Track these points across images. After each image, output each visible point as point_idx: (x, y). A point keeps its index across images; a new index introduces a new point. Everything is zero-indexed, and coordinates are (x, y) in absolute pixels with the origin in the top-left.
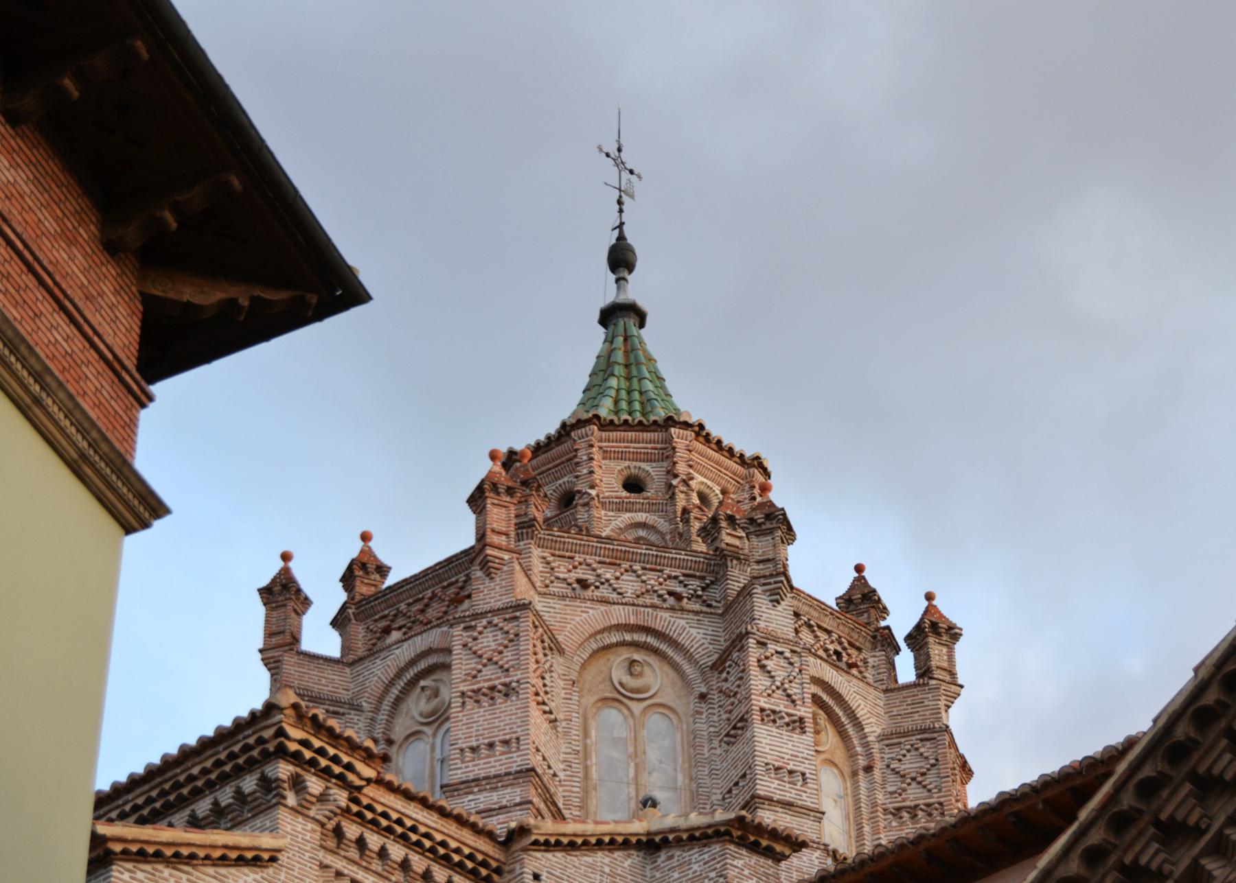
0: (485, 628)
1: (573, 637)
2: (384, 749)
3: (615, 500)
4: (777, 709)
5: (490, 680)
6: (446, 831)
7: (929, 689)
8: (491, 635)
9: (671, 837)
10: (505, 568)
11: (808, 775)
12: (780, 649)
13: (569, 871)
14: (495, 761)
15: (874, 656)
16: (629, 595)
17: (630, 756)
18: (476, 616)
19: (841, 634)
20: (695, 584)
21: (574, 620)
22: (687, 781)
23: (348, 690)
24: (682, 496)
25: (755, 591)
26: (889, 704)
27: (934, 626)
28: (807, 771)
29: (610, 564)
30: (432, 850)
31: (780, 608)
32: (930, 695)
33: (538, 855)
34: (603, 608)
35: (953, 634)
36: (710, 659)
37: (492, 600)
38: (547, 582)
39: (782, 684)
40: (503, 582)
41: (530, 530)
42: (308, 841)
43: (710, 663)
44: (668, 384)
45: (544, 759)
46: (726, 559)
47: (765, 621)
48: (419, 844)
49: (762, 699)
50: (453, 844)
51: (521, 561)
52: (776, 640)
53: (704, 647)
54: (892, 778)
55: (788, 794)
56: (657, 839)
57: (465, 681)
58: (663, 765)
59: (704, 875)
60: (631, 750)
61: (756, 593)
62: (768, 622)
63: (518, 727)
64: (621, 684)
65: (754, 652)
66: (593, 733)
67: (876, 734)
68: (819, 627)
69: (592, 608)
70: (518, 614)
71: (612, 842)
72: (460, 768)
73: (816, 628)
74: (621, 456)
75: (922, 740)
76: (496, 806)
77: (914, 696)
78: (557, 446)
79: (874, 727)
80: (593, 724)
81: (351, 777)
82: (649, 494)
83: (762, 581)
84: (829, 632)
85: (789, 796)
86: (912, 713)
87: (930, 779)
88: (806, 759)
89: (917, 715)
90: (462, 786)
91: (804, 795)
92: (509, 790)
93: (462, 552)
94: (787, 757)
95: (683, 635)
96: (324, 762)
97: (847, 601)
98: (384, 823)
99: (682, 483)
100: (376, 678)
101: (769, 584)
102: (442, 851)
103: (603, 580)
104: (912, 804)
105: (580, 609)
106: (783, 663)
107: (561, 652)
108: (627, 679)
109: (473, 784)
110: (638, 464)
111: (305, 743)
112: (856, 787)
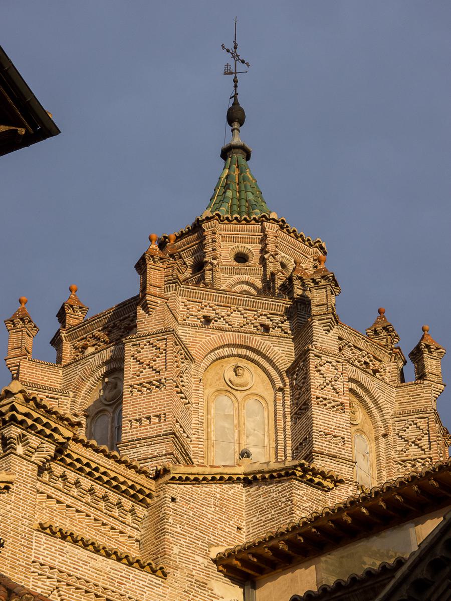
1: (201, 352)
3: (229, 267)
4: (327, 397)
5: (148, 378)
7: (424, 387)
8: (148, 350)
9: (258, 476)
12: (329, 360)
13: (194, 496)
14: (150, 428)
16: (236, 326)
17: (236, 426)
19: (369, 352)
20: (278, 319)
21: (201, 341)
23: (61, 384)
24: (271, 265)
25: (314, 324)
26: (398, 396)
28: (345, 436)
30: (108, 482)
31: (330, 334)
32: (424, 390)
33: (175, 486)
34: (219, 333)
36: (286, 366)
37: (150, 328)
38: (185, 317)
39: (330, 382)
40: (157, 317)
41: (174, 285)
42: (29, 477)
43: (285, 369)
45: (181, 427)
46: (297, 304)
47: (320, 343)
48: (99, 478)
49: (318, 391)
50: (122, 479)
51: (169, 304)
53: (282, 358)
54: (400, 441)
55: (333, 451)
56: (250, 477)
58: (256, 432)
59: (278, 500)
60: (236, 422)
61: (315, 325)
62: (322, 343)
63: (165, 407)
64: (230, 381)
66: (213, 411)
67: (390, 414)
68: (355, 347)
69: (213, 334)
70: (166, 337)
71: (221, 478)
72: (129, 432)
73: (353, 348)
74: (234, 240)
75: (419, 418)
76: (151, 456)
77: (415, 390)
79: (389, 412)
80: (213, 405)
81: (56, 436)
82: (250, 264)
83: (319, 317)
84: (361, 350)
86: (413, 401)
88: (345, 429)
89: (416, 402)
90: (129, 444)
91: (343, 451)
92: (159, 445)
93: (132, 298)
94: (333, 427)
95: (269, 351)
96: (40, 427)
98: (78, 465)
99: (271, 257)
100: (77, 377)
101: (324, 319)
102: (115, 483)
103: (220, 316)
105: (205, 334)
106: (332, 369)
107: (193, 360)
109: (136, 442)
110: (244, 245)
111: (27, 415)
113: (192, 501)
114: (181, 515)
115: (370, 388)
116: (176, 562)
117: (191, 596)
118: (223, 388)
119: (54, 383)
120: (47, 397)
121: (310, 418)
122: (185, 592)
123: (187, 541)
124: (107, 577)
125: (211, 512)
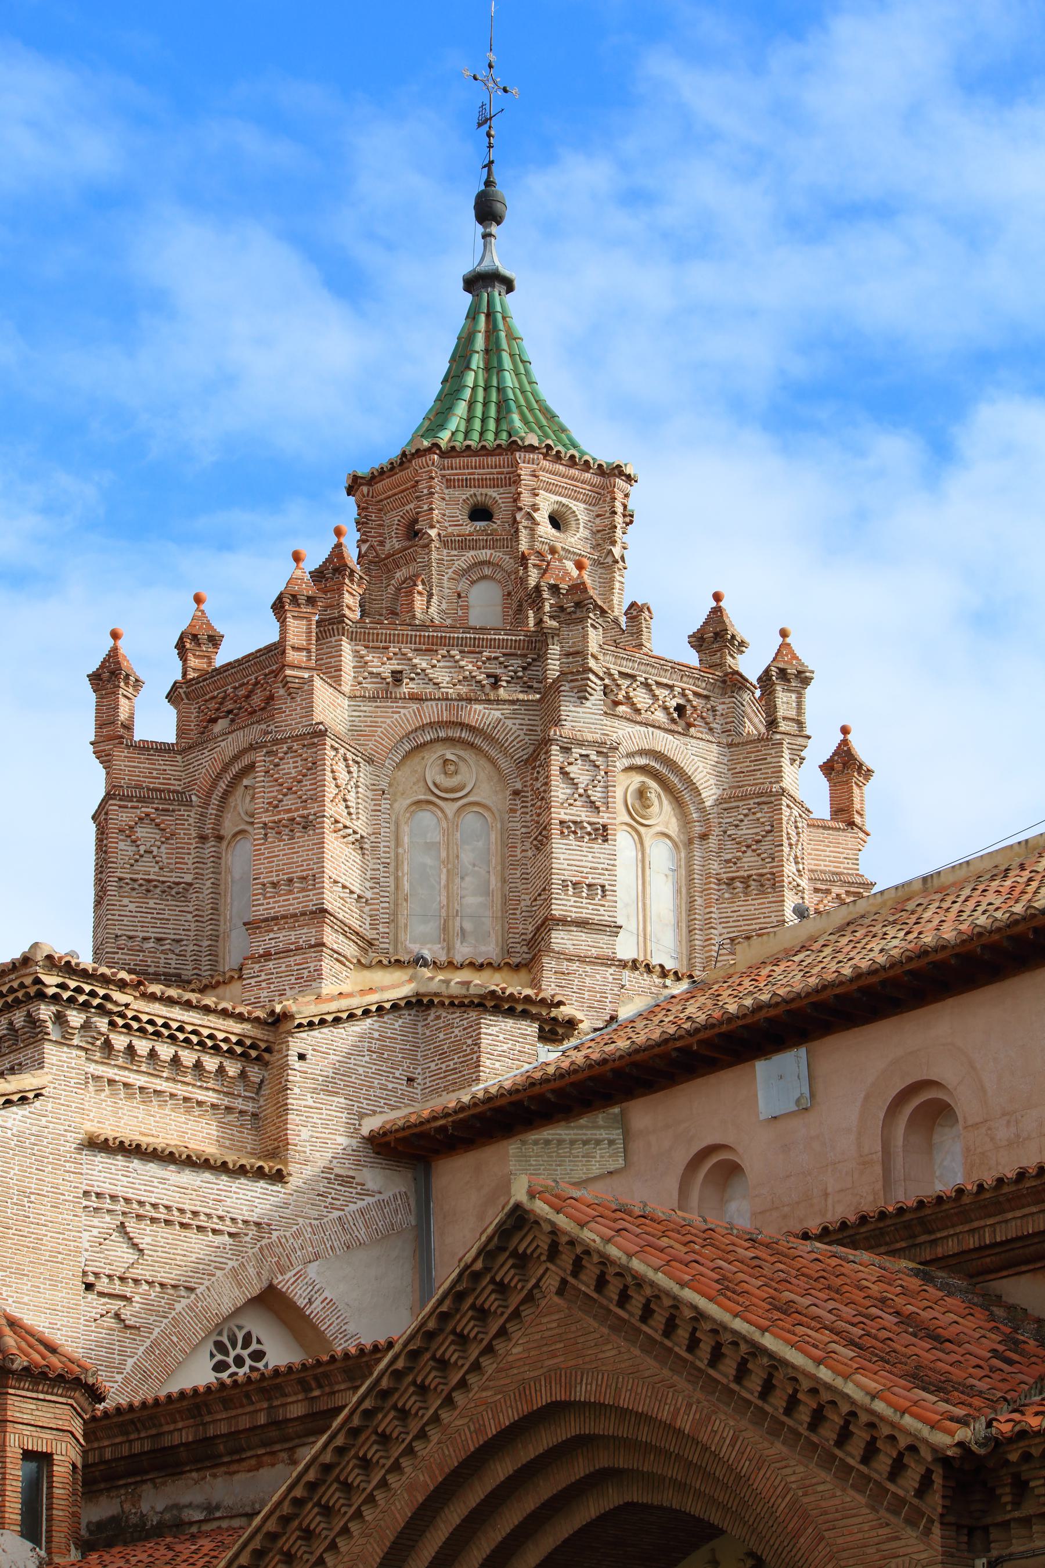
0: (286, 753)
2: (214, 846)
4: (578, 819)
6: (212, 1025)
8: (291, 761)
10: (306, 687)
11: (607, 887)
12: (584, 752)
14: (294, 899)
15: (724, 703)
18: (276, 742)
20: (515, 663)
22: (499, 885)
23: (180, 780)
25: (562, 688)
27: (783, 673)
28: (606, 883)
29: (426, 650)
31: (588, 704)
32: (773, 751)
33: (304, 1035)
35: (804, 679)
36: (525, 752)
39: (585, 791)
41: (340, 626)
42: (73, 1068)
44: (534, 369)
49: (562, 811)
52: (581, 744)
53: (519, 739)
54: (729, 844)
55: (584, 911)
57: (267, 811)
58: (476, 869)
60: (444, 854)
63: (314, 864)
64: (435, 784)
65: (557, 758)
66: (406, 839)
69: (404, 707)
71: (380, 1009)
72: (262, 904)
74: (467, 484)
75: (759, 804)
77: (758, 751)
78: (401, 471)
79: (710, 794)
80: (405, 829)
81: (109, 1006)
84: (671, 687)
85: (585, 914)
87: (765, 846)
88: (607, 870)
89: (759, 773)
91: (602, 908)
94: (585, 870)
96: (82, 998)
97: (698, 641)
100: (204, 770)
101: (576, 680)
104: (746, 874)
105: (390, 710)
108: (441, 779)
110: (484, 491)
111: (63, 986)
112: (690, 859)
113: (331, 1052)
114: (313, 1079)
115: (678, 758)
116: (305, 1152)
117: (329, 1200)
118: (422, 797)
119: (170, 779)
120: (157, 809)
121: (549, 856)
122: (318, 1195)
123: (324, 1116)
124: (197, 1195)
125: (363, 1063)
